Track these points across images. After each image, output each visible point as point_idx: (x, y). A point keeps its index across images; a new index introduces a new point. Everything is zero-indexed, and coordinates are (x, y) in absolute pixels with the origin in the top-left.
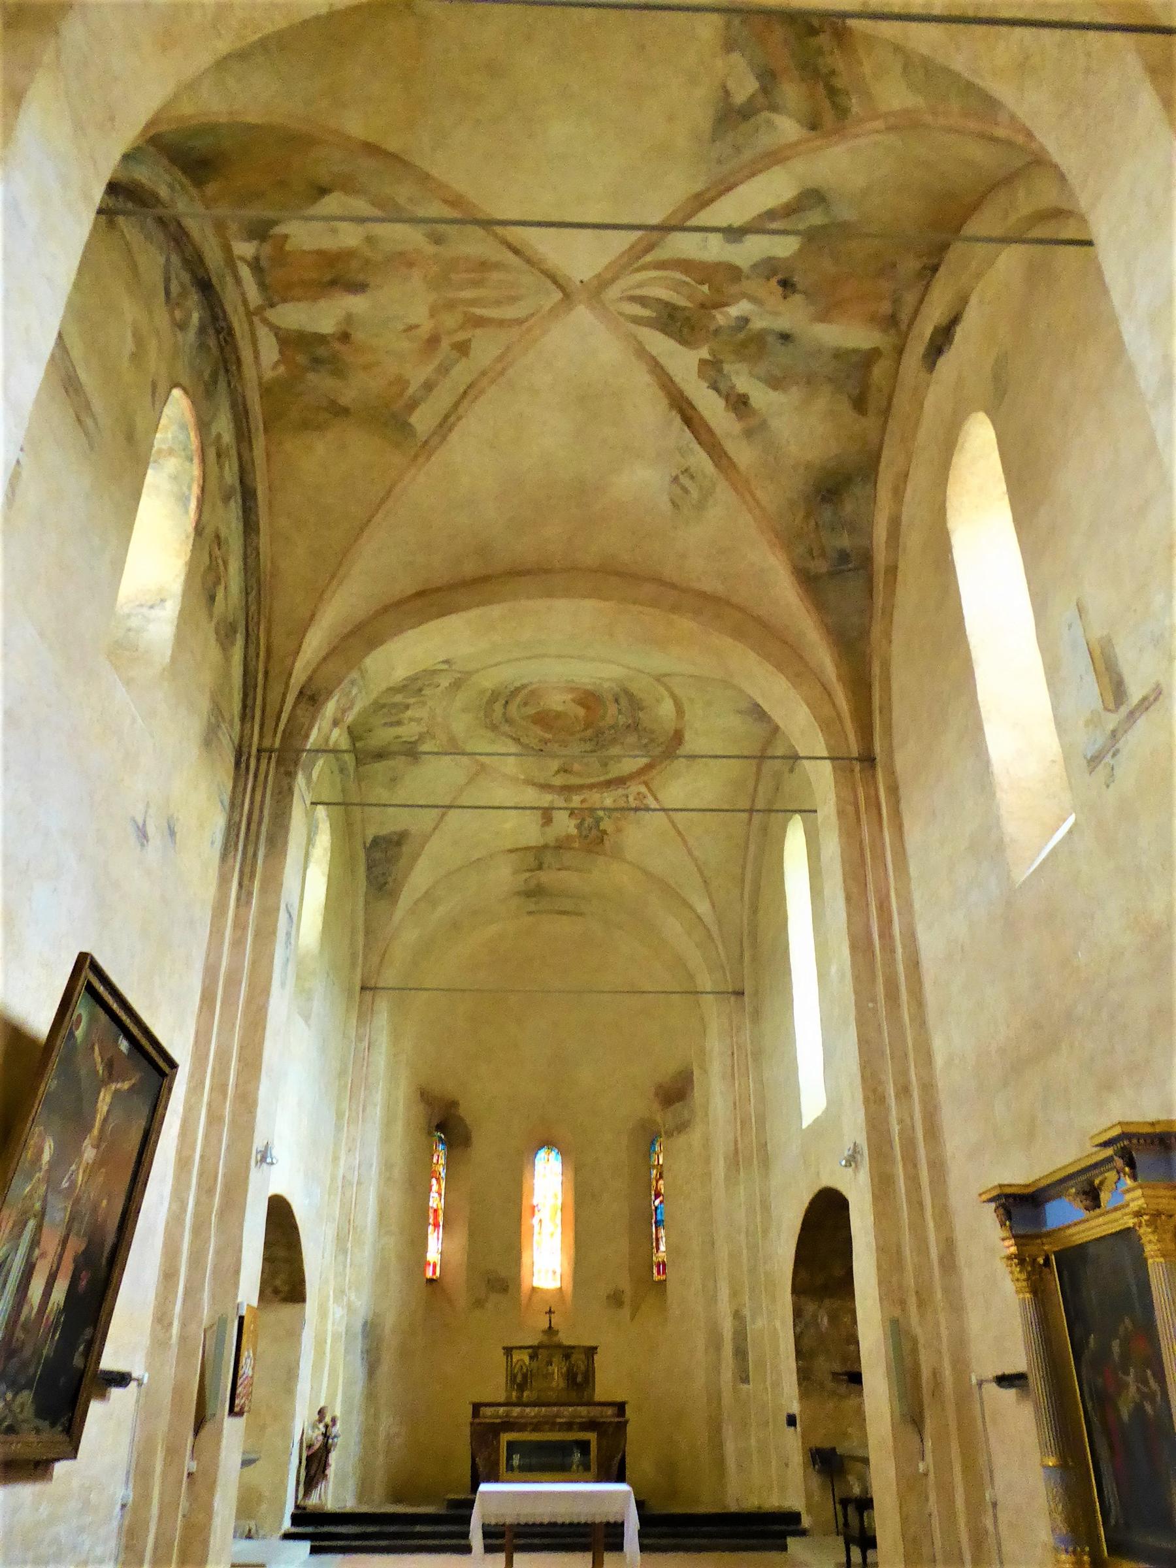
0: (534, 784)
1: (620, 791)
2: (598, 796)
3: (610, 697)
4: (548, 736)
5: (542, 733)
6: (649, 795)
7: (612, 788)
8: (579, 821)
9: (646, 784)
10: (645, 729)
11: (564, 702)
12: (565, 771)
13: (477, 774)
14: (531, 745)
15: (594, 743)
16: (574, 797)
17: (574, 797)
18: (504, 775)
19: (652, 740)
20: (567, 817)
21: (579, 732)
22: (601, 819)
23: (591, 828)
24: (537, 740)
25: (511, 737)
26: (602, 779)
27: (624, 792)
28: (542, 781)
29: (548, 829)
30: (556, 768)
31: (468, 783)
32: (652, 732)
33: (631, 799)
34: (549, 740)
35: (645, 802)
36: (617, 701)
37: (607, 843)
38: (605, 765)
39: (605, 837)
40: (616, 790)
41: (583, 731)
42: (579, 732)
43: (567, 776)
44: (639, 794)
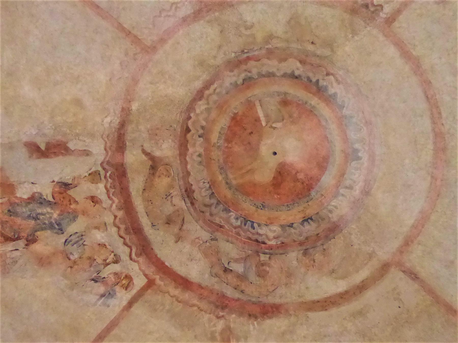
0: (122, 125)
1: (123, 251)
2: (109, 219)
3: (310, 212)
4: (214, 137)
5: (217, 129)
6: (134, 291)
7: (127, 238)
8: (50, 198)
9: (150, 284)
10: (263, 265)
11: (275, 153)
12: (153, 168)
13: (136, 40)
14: (192, 115)
15: (207, 201)
16: (101, 186)
17: (101, 186)
18: (135, 81)
19: (242, 277)
20: (56, 179)
21: (226, 178)
22: (61, 231)
23: (36, 219)
24: (204, 123)
25: (207, 86)
26: (145, 221)
27: (125, 257)
28: (129, 137)
29: (23, 153)
30: (157, 153)
31: (121, 27)
32: (262, 275)
33: (116, 268)
34: (207, 140)
35: (117, 288)
36: (307, 220)
37: (10, 246)
38: (169, 222)
39: (21, 243)
40: (125, 244)
41: (227, 183)
42: (226, 178)
43: (146, 170)
44: (128, 277)
